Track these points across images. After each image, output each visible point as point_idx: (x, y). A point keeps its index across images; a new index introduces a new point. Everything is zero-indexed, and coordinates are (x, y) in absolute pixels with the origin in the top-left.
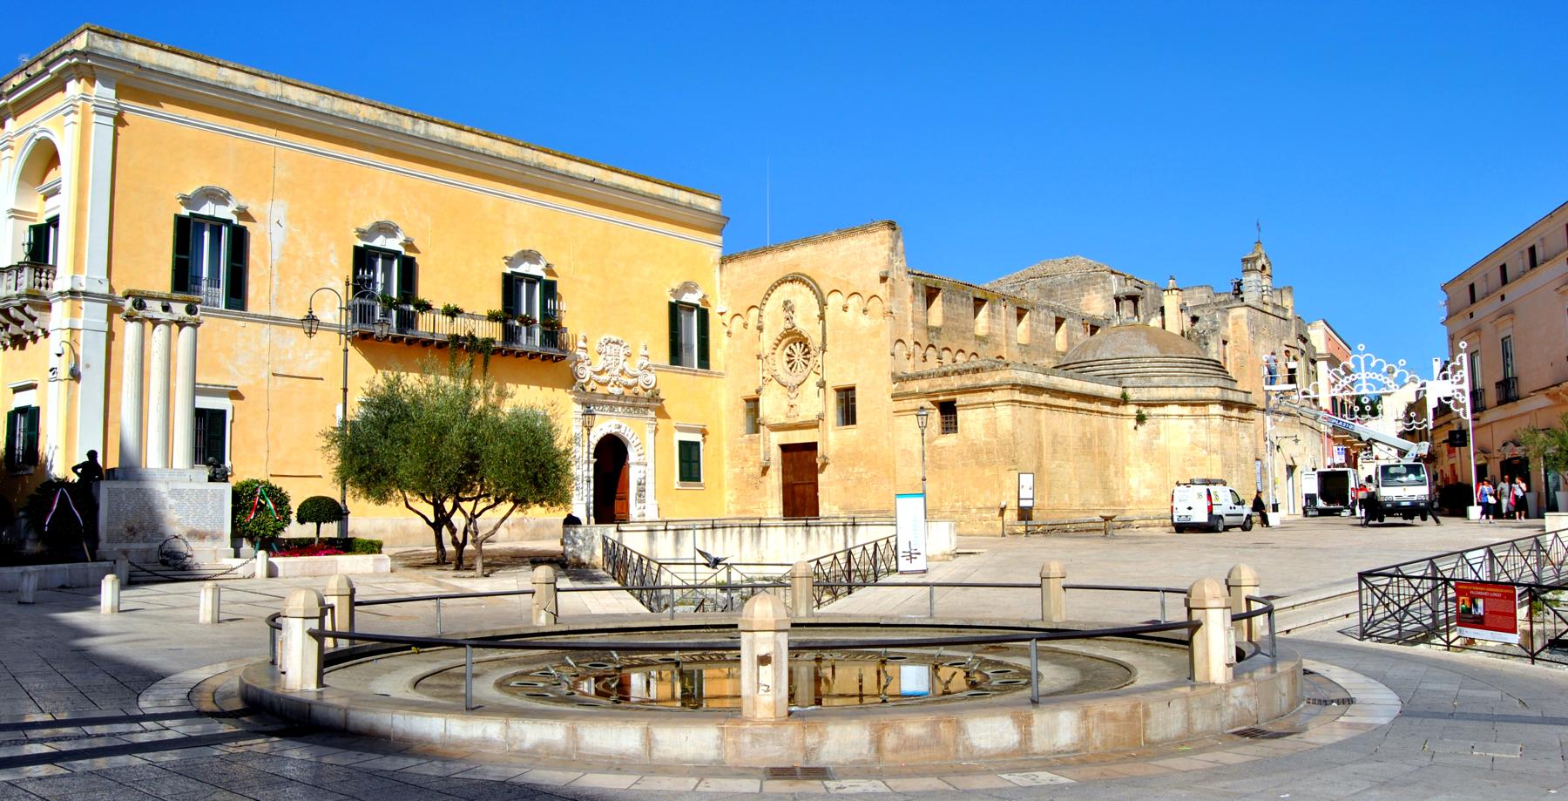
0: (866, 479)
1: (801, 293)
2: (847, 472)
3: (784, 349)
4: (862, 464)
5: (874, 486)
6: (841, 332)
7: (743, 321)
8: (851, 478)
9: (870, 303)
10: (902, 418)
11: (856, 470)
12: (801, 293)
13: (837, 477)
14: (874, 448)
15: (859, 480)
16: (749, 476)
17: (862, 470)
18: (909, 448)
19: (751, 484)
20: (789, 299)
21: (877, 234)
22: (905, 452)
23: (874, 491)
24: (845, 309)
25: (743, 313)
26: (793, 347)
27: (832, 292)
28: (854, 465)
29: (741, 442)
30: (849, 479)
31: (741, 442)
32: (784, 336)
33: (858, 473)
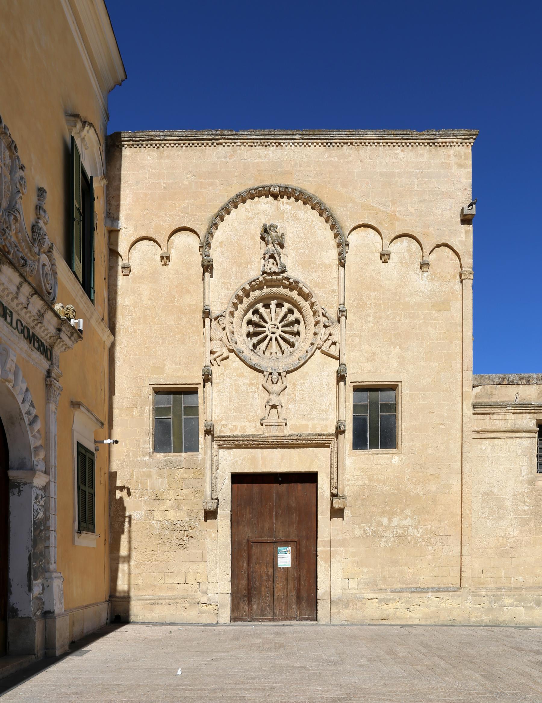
0: (414, 537)
1: (295, 217)
2: (379, 524)
3: (246, 312)
4: (408, 512)
5: (430, 548)
6: (373, 294)
7: (159, 252)
8: (385, 535)
9: (433, 256)
10: (487, 442)
11: (396, 521)
12: (295, 217)
13: (358, 532)
14: (433, 487)
15: (402, 538)
16: (163, 526)
17: (406, 522)
18: (495, 490)
19: (169, 540)
20: (276, 223)
21: (451, 151)
22: (488, 495)
23: (430, 557)
24: (384, 257)
25: (162, 240)
26: (262, 310)
27: (359, 226)
28: (391, 514)
29: (148, 465)
30: (381, 537)
31: (148, 465)
32: (256, 285)
33: (399, 526)
